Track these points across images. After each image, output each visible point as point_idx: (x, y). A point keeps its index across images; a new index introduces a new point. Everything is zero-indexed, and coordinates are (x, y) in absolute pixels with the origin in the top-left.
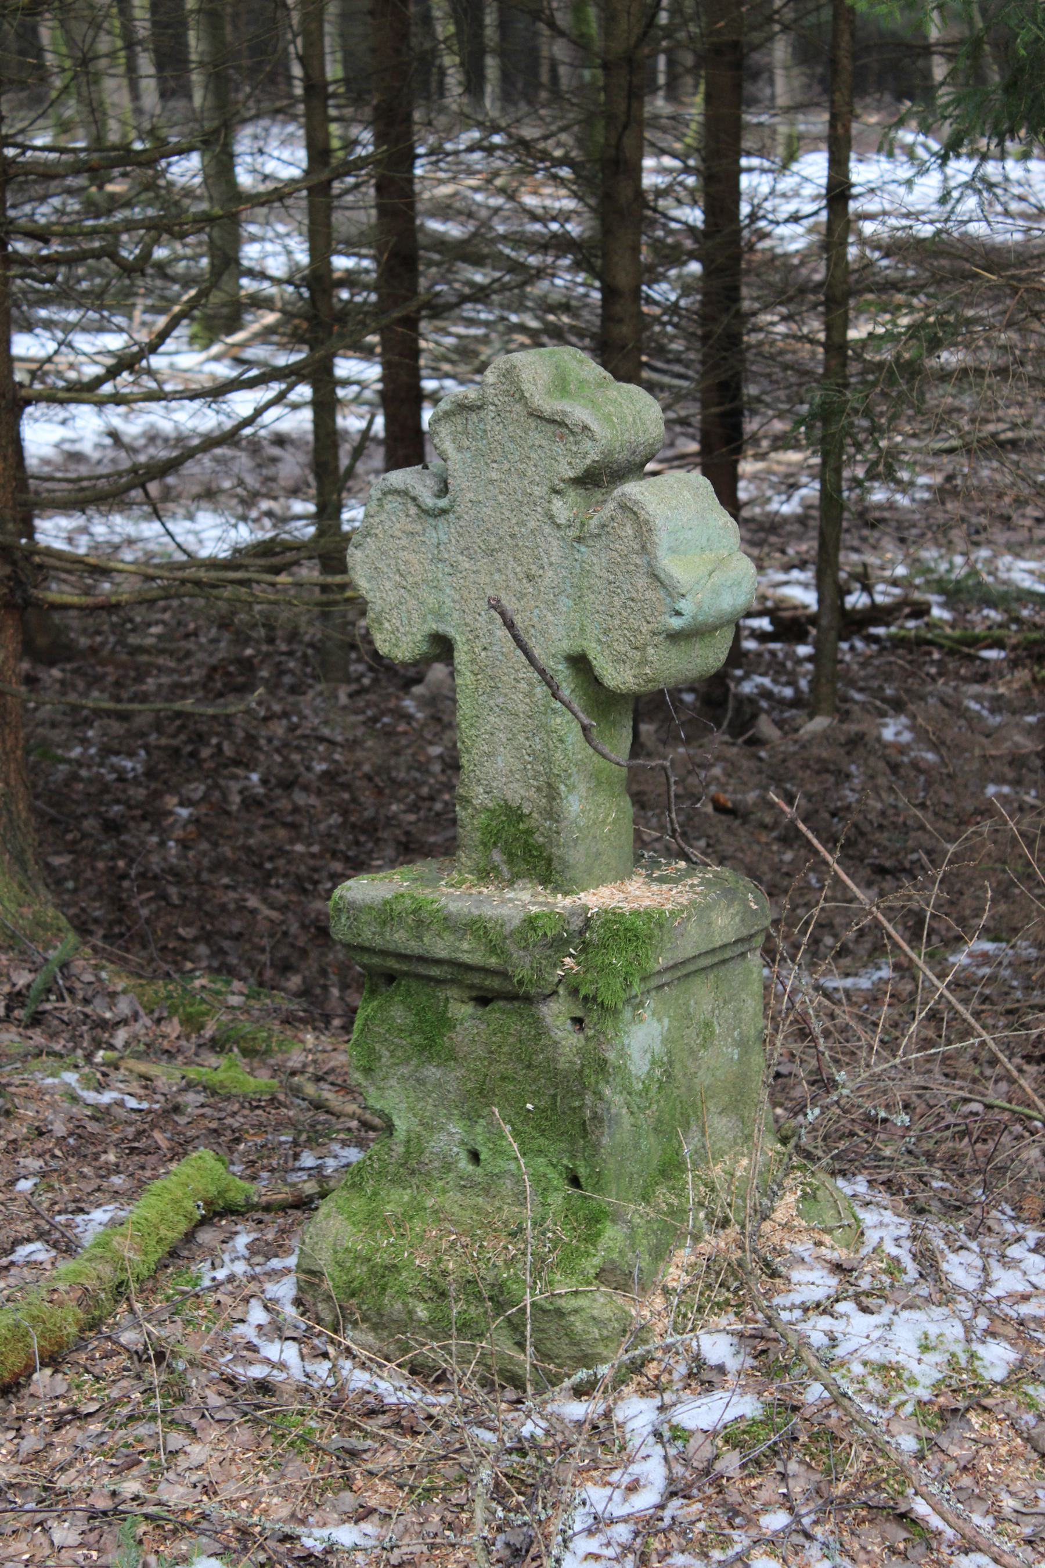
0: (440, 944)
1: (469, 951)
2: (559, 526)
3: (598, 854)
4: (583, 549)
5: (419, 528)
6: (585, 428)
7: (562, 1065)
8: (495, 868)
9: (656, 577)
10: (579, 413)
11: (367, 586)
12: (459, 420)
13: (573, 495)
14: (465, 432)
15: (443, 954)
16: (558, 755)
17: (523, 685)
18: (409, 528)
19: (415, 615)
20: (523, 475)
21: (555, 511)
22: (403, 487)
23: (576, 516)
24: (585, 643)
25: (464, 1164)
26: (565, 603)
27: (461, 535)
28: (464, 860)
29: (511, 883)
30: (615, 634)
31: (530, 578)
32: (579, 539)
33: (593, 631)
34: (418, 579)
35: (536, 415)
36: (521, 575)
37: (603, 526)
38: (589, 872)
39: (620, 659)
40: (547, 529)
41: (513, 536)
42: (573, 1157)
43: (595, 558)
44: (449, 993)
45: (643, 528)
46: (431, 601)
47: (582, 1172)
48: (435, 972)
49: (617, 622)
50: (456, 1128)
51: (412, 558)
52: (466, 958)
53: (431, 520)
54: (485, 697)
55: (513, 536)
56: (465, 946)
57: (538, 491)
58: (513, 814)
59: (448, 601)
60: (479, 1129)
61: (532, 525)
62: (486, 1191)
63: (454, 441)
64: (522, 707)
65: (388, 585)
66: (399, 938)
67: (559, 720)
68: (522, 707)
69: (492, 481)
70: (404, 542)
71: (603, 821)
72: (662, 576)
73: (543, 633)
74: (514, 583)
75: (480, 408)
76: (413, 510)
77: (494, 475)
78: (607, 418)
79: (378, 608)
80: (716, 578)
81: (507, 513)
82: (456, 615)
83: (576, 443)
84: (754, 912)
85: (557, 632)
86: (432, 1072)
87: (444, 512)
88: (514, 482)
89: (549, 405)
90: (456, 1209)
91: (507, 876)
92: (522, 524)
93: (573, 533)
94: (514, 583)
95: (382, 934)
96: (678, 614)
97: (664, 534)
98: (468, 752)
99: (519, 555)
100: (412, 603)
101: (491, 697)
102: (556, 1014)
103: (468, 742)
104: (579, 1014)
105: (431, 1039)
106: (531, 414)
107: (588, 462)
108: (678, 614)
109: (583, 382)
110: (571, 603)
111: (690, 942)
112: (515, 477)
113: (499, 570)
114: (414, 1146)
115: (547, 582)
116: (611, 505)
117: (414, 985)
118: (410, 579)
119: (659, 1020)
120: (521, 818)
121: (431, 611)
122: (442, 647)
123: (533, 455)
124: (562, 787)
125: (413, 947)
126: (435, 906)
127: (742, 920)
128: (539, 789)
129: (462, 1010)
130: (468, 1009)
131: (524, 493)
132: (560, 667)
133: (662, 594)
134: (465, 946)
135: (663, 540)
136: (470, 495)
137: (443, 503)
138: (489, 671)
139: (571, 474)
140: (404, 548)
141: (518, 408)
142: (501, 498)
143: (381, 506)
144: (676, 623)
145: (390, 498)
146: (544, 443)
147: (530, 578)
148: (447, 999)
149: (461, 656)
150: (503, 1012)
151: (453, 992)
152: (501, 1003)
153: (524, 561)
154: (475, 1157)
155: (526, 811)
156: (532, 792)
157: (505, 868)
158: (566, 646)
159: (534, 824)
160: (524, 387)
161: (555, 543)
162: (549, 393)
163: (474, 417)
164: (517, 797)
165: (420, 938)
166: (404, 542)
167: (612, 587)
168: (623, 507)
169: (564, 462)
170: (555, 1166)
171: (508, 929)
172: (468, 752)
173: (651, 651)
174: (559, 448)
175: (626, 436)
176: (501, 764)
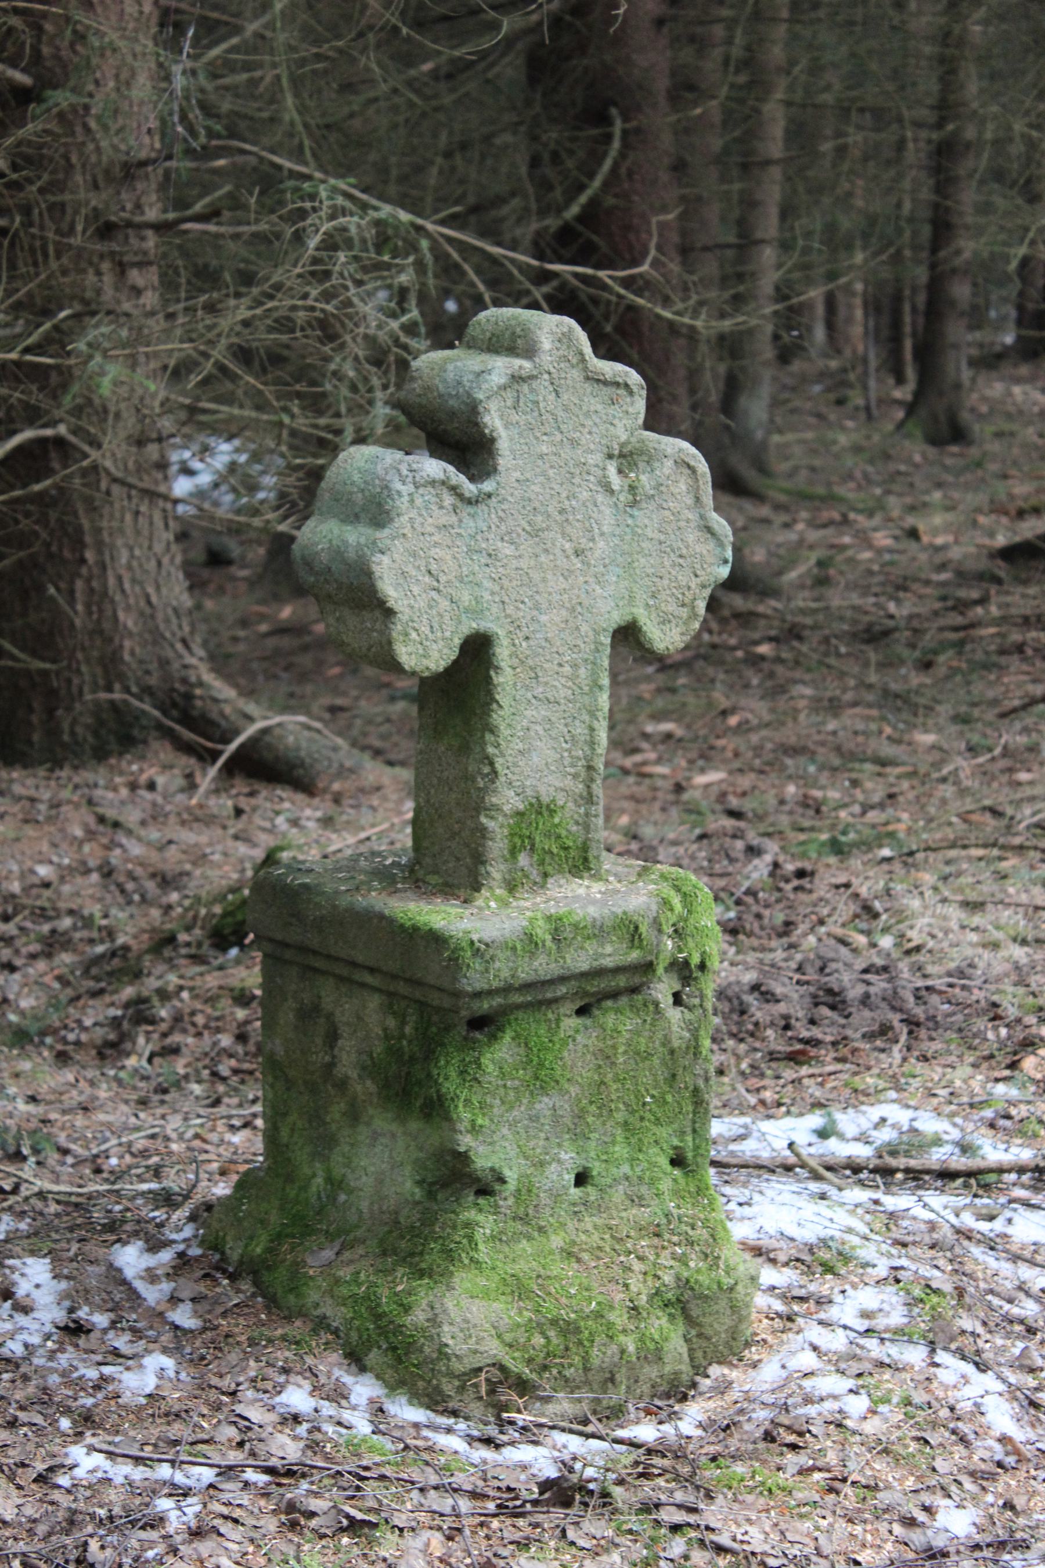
4: (636, 513)
5: (454, 519)
7: (676, 1043)
12: (509, 395)
17: (567, 669)
18: (443, 520)
24: (635, 610)
27: (501, 519)
30: (663, 596)
33: (641, 596)
34: (451, 577)
36: (570, 552)
40: (600, 498)
46: (466, 598)
52: (608, 962)
55: (562, 511)
56: (609, 949)
59: (487, 596)
60: (593, 1144)
61: (585, 495)
63: (501, 417)
64: (564, 693)
66: (543, 966)
69: (541, 456)
74: (562, 562)
76: (448, 500)
77: (544, 449)
81: (557, 487)
86: (544, 1104)
88: (566, 453)
98: (503, 755)
99: (568, 529)
100: (445, 604)
106: (588, 378)
113: (546, 551)
114: (525, 1191)
115: (598, 553)
117: (520, 1014)
118: (443, 578)
121: (467, 611)
128: (575, 776)
133: (712, 545)
134: (609, 949)
136: (517, 475)
138: (530, 662)
140: (436, 544)
142: (551, 472)
146: (599, 407)
149: (502, 653)
154: (581, 1179)
156: (569, 782)
161: (608, 511)
163: (525, 388)
166: (436, 538)
167: (663, 547)
172: (503, 755)
176: (535, 759)
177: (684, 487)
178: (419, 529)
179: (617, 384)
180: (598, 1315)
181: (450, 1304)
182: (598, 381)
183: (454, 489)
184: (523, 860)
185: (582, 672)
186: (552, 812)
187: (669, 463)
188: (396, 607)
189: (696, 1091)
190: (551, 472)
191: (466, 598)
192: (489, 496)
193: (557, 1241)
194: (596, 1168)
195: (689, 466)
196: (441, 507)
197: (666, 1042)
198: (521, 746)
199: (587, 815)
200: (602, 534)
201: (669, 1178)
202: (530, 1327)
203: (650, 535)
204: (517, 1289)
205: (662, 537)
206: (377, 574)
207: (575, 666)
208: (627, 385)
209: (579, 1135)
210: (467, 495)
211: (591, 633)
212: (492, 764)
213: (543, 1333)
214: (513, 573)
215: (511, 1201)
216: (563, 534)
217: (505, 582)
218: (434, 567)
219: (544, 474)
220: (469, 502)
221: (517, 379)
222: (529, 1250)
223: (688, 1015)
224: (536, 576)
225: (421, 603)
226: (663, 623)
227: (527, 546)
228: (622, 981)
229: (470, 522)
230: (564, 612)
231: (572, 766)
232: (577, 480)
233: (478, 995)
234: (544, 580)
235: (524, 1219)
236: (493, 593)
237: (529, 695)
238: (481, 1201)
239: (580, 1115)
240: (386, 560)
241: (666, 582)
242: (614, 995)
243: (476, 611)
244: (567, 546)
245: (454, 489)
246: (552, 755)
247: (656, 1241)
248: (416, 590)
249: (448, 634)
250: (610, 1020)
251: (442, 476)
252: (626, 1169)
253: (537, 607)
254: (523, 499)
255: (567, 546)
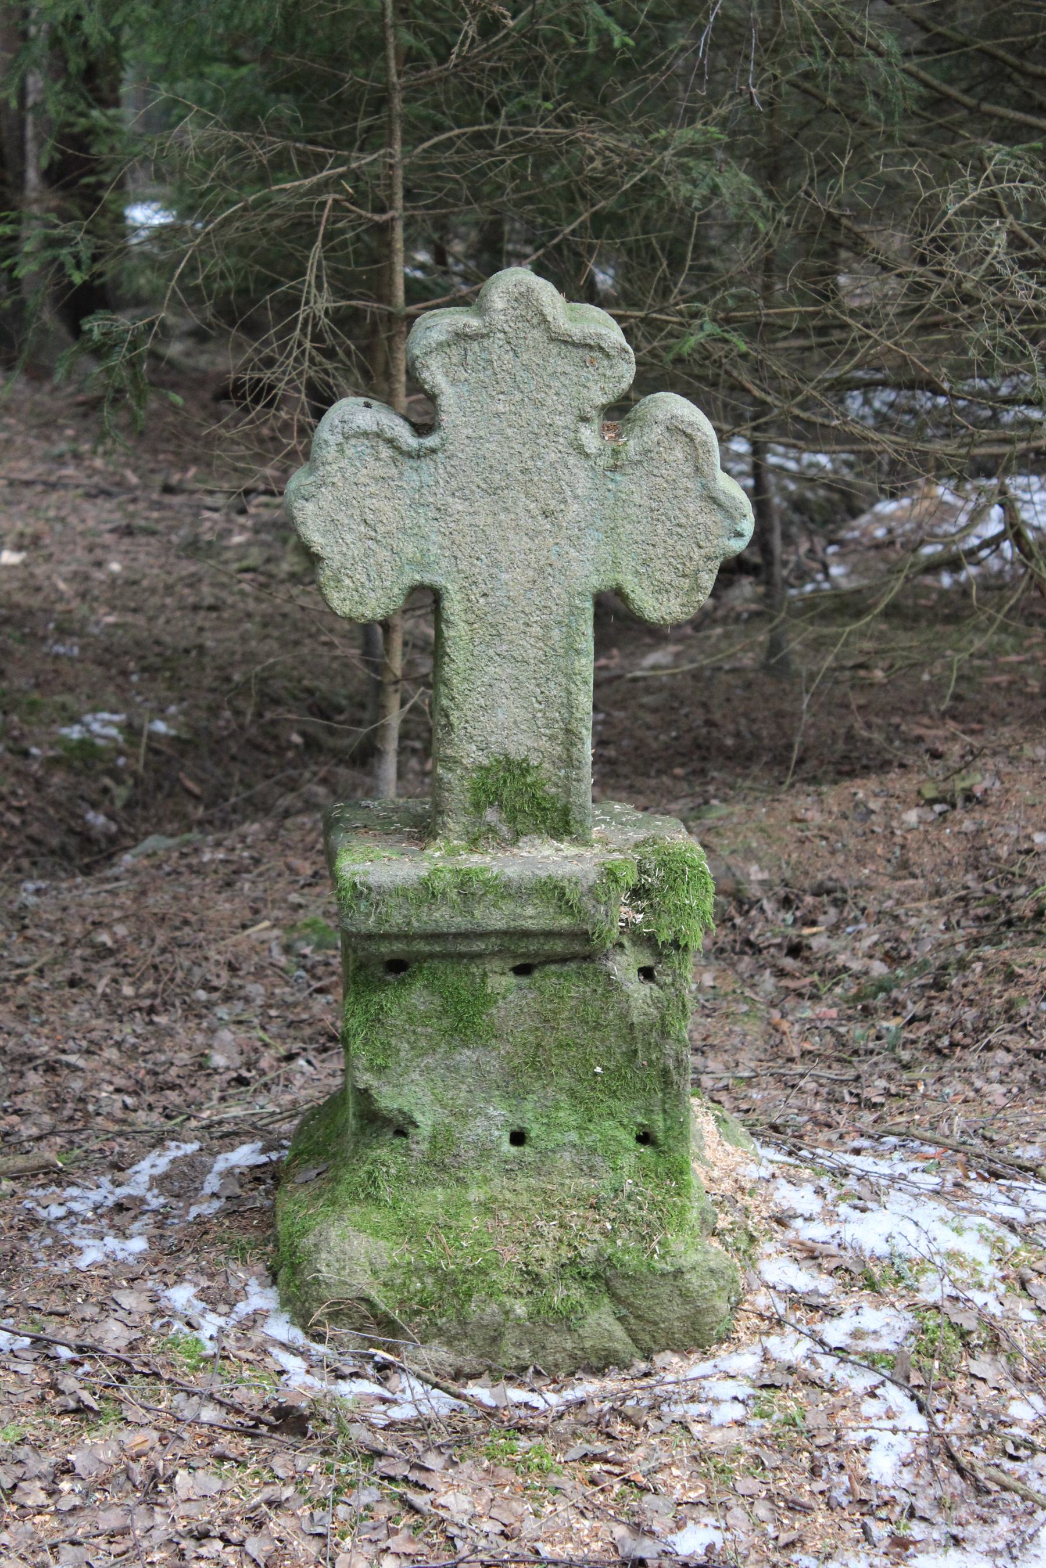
0: (496, 914)
1: (533, 916)
4: (618, 478)
5: (394, 471)
7: (635, 1018)
8: (491, 830)
9: (714, 500)
11: (321, 541)
12: (455, 353)
14: (464, 364)
17: (536, 630)
18: (380, 472)
19: (387, 567)
24: (620, 577)
25: (507, 1148)
27: (451, 475)
28: (451, 825)
29: (515, 842)
31: (545, 514)
33: (628, 563)
34: (392, 528)
35: (567, 342)
39: (661, 590)
40: (571, 461)
42: (649, 1112)
43: (634, 487)
44: (488, 967)
46: (410, 550)
47: (659, 1125)
48: (479, 946)
49: (660, 551)
50: (498, 1111)
51: (386, 507)
52: (529, 924)
54: (483, 647)
56: (530, 911)
57: (559, 421)
58: (515, 769)
59: (435, 550)
60: (529, 1106)
61: (553, 456)
62: (538, 1171)
64: (532, 653)
66: (443, 917)
67: (583, 661)
68: (532, 653)
69: (497, 415)
70: (373, 488)
72: (722, 497)
74: (525, 521)
76: (385, 452)
77: (501, 408)
79: (336, 565)
81: (518, 447)
82: (444, 563)
86: (466, 1056)
88: (529, 412)
90: (509, 1195)
91: (509, 836)
94: (525, 521)
98: (458, 708)
99: (533, 490)
100: (383, 554)
102: (624, 966)
103: (459, 698)
104: (648, 961)
105: (463, 1023)
106: (552, 340)
108: (739, 535)
110: (601, 536)
112: (530, 408)
115: (570, 516)
117: (439, 966)
118: (381, 529)
120: (525, 771)
121: (410, 562)
122: (427, 600)
125: (461, 923)
128: (552, 738)
129: (501, 982)
130: (511, 980)
131: (541, 425)
133: (719, 516)
134: (530, 911)
138: (490, 619)
140: (371, 496)
141: (537, 333)
142: (509, 432)
143: (342, 451)
146: (569, 369)
148: (485, 975)
149: (453, 606)
150: (559, 976)
151: (495, 965)
152: (553, 967)
153: (541, 497)
154: (518, 1138)
156: (544, 743)
157: (504, 829)
161: (582, 474)
163: (475, 346)
164: (523, 749)
166: (373, 488)
170: (624, 1127)
171: (586, 884)
172: (458, 708)
176: (501, 717)
177: (680, 456)
178: (352, 479)
179: (591, 347)
180: (482, 1271)
181: (334, 1233)
182: (565, 342)
183: (391, 442)
184: (491, 815)
185: (556, 634)
186: (525, 771)
187: (659, 429)
188: (323, 553)
189: (665, 1072)
190: (509, 432)
191: (410, 550)
192: (433, 451)
193: (475, 1194)
194: (535, 1130)
195: (687, 435)
196: (378, 459)
197: (623, 1016)
198: (482, 702)
199: (567, 778)
200: (576, 497)
201: (631, 1156)
202: (412, 1271)
203: (638, 501)
204: (411, 1231)
205: (654, 505)
206: (299, 520)
207: (546, 627)
208: (601, 349)
209: (516, 1095)
210: (405, 448)
211: (564, 596)
212: (447, 716)
213: (420, 1279)
214: (466, 530)
215: (425, 1146)
216: (527, 495)
217: (458, 538)
218: (370, 517)
219: (501, 432)
220: (409, 455)
221: (461, 337)
222: (440, 1198)
223: (657, 992)
224: (493, 533)
225: (356, 551)
226: (659, 592)
227: (483, 503)
228: (559, 946)
229: (412, 476)
230: (531, 573)
231: (547, 727)
232: (543, 441)
233: (370, 937)
234: (504, 538)
235: (443, 1168)
236: (442, 548)
237: (491, 652)
238: (397, 1141)
239: (514, 1073)
240: (310, 507)
241: (660, 551)
242: (563, 960)
243: (422, 565)
244: (532, 506)
245: (391, 442)
246: (522, 715)
247: (592, 1214)
248: (349, 538)
249: (388, 584)
250: (550, 984)
251: (375, 428)
252: (573, 1136)
253: (496, 564)
254: (476, 455)
255: (532, 506)
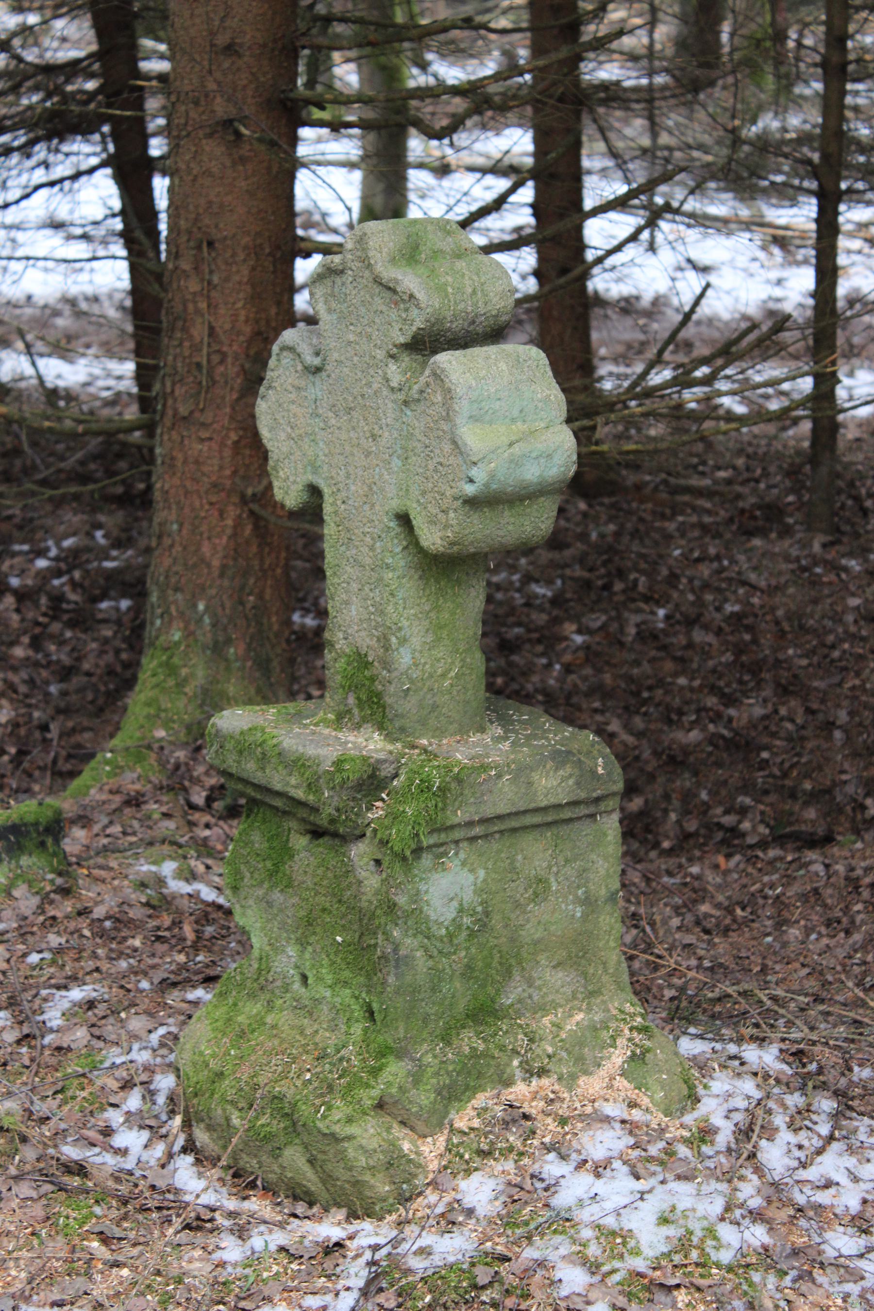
2: (392, 389)
3: (435, 707)
4: (409, 413)
6: (412, 296)
9: (454, 442)
10: (410, 281)
13: (406, 359)
15: (278, 787)
16: (390, 609)
17: (368, 539)
18: (296, 382)
20: (369, 337)
21: (390, 375)
22: (291, 344)
23: (408, 380)
24: (408, 503)
26: (396, 463)
30: (429, 496)
31: (374, 437)
32: (406, 403)
33: (415, 492)
35: (377, 281)
37: (422, 392)
38: (423, 722)
41: (363, 396)
42: (368, 992)
45: (448, 394)
46: (310, 453)
51: (299, 411)
53: (311, 377)
54: (343, 548)
55: (363, 396)
56: (293, 781)
61: (375, 386)
63: (326, 302)
65: (283, 436)
66: (250, 768)
67: (390, 575)
68: (368, 561)
69: (350, 343)
71: (443, 676)
73: (382, 490)
75: (342, 272)
77: (351, 337)
78: (441, 289)
79: (275, 457)
80: (516, 449)
82: (326, 468)
83: (406, 310)
84: (599, 777)
85: (391, 491)
86: (277, 896)
87: (318, 370)
89: (389, 273)
92: (369, 385)
93: (401, 396)
94: (363, 441)
95: (239, 762)
96: (471, 481)
97: (465, 403)
101: (348, 549)
104: (379, 857)
107: (414, 329)
108: (471, 481)
109: (437, 253)
110: (400, 464)
111: (504, 797)
113: (354, 428)
116: (427, 372)
119: (472, 871)
120: (367, 665)
123: (377, 320)
124: (394, 640)
125: (259, 778)
126: (275, 741)
127: (578, 783)
128: (378, 640)
129: (300, 842)
132: (392, 524)
135: (463, 408)
136: (336, 355)
137: (317, 361)
139: (402, 340)
140: (293, 402)
141: (367, 274)
142: (356, 359)
144: (470, 490)
145: (285, 353)
147: (374, 437)
151: (293, 824)
155: (370, 659)
157: (356, 711)
158: (395, 504)
159: (375, 672)
160: (371, 254)
161: (390, 405)
162: (393, 261)
163: (338, 281)
165: (263, 769)
166: (293, 396)
168: (434, 374)
169: (397, 327)
170: (357, 998)
173: (452, 515)
174: (393, 315)
175: (461, 306)
198: (344, 596)
